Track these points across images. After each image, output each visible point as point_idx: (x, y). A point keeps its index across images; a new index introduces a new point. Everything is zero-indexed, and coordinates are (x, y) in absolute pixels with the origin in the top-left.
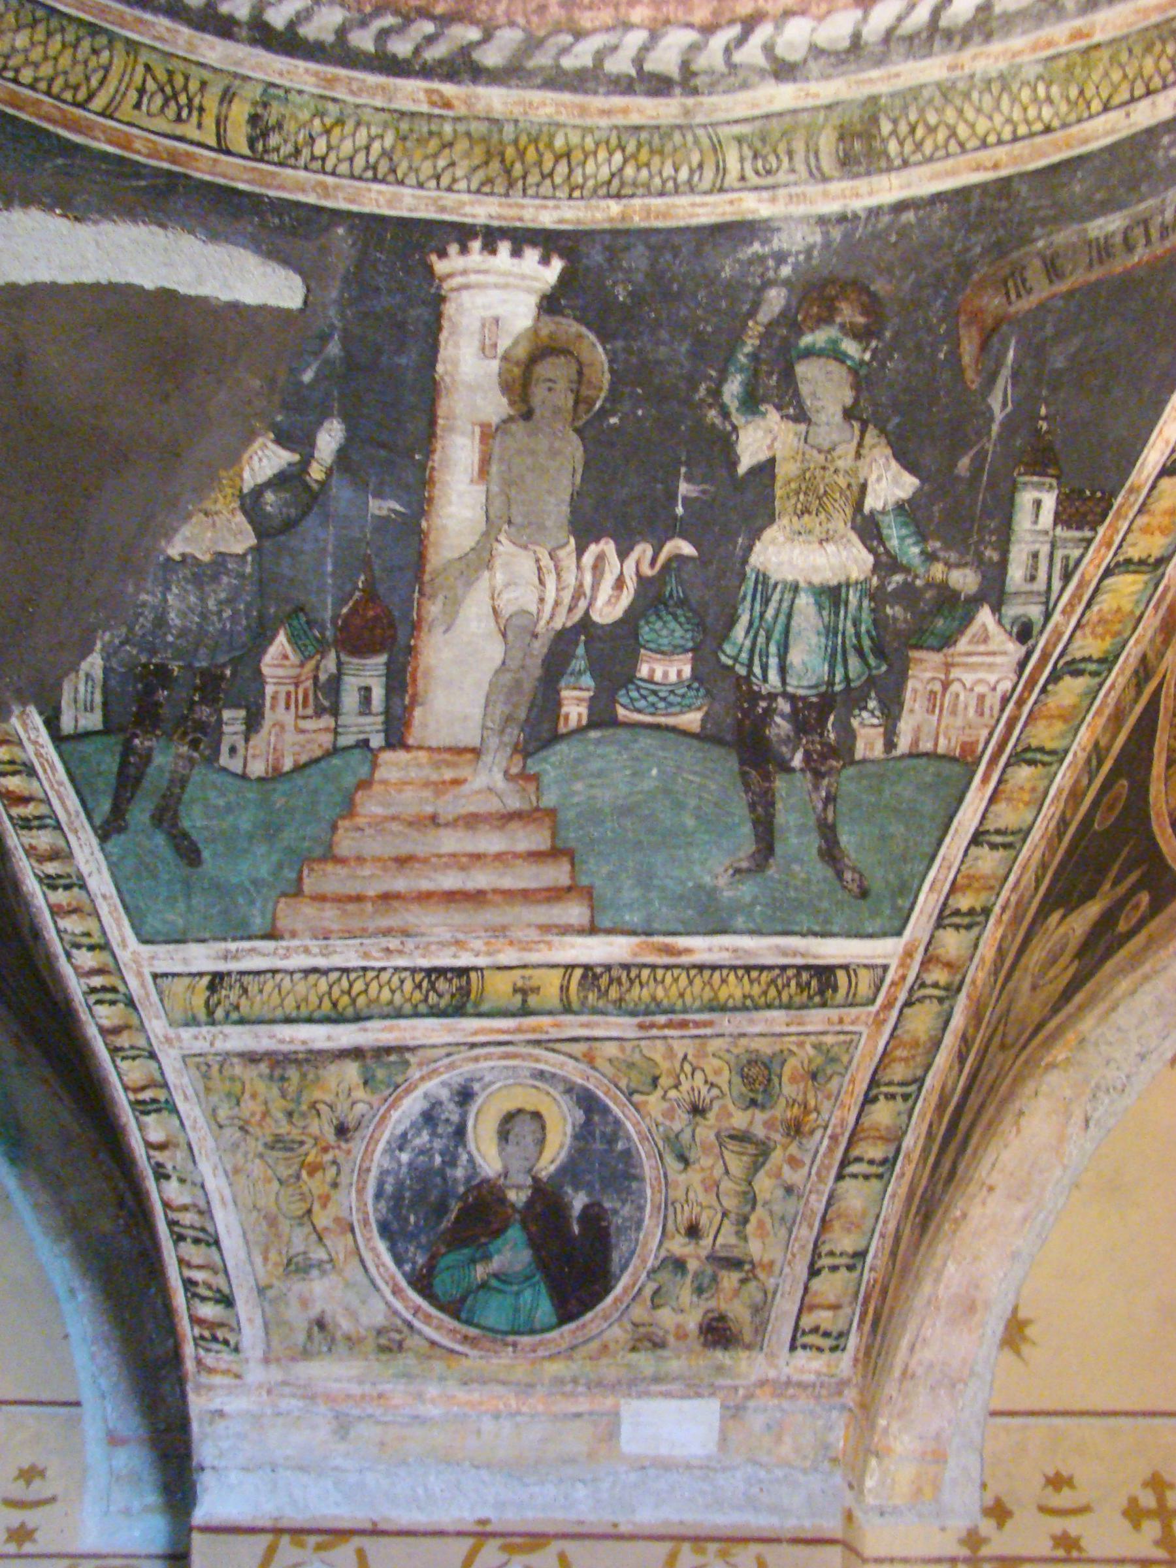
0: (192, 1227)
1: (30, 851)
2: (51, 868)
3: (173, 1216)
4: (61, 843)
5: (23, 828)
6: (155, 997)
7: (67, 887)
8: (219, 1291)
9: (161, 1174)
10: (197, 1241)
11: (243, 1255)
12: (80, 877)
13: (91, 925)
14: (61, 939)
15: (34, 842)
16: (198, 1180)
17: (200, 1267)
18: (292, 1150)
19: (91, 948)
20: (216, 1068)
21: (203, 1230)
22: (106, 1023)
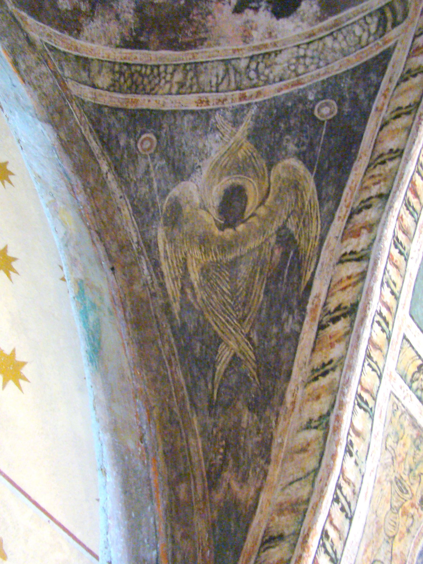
0: (345, 498)
1: (400, 218)
2: (401, 237)
3: (342, 482)
4: (412, 231)
5: (406, 205)
6: (398, 348)
7: (401, 253)
8: (335, 553)
9: (349, 452)
10: (343, 509)
11: (358, 540)
12: (408, 255)
13: (398, 281)
14: (384, 273)
15: (404, 217)
16: (363, 470)
17: (335, 528)
18: (402, 492)
19: (393, 293)
20: (399, 413)
21: (349, 504)
22: (375, 339)
